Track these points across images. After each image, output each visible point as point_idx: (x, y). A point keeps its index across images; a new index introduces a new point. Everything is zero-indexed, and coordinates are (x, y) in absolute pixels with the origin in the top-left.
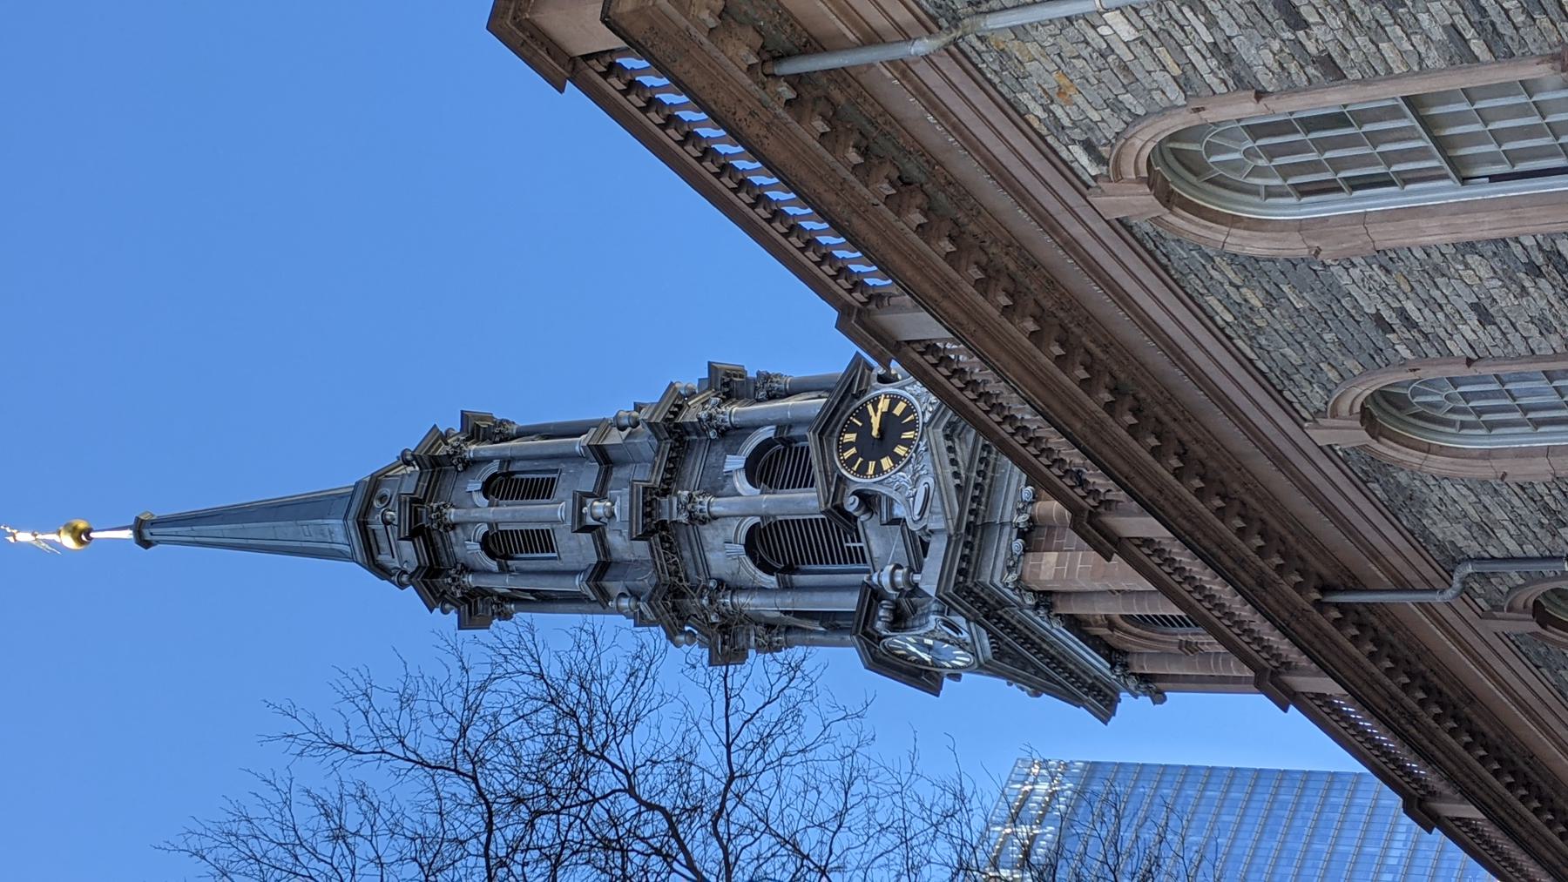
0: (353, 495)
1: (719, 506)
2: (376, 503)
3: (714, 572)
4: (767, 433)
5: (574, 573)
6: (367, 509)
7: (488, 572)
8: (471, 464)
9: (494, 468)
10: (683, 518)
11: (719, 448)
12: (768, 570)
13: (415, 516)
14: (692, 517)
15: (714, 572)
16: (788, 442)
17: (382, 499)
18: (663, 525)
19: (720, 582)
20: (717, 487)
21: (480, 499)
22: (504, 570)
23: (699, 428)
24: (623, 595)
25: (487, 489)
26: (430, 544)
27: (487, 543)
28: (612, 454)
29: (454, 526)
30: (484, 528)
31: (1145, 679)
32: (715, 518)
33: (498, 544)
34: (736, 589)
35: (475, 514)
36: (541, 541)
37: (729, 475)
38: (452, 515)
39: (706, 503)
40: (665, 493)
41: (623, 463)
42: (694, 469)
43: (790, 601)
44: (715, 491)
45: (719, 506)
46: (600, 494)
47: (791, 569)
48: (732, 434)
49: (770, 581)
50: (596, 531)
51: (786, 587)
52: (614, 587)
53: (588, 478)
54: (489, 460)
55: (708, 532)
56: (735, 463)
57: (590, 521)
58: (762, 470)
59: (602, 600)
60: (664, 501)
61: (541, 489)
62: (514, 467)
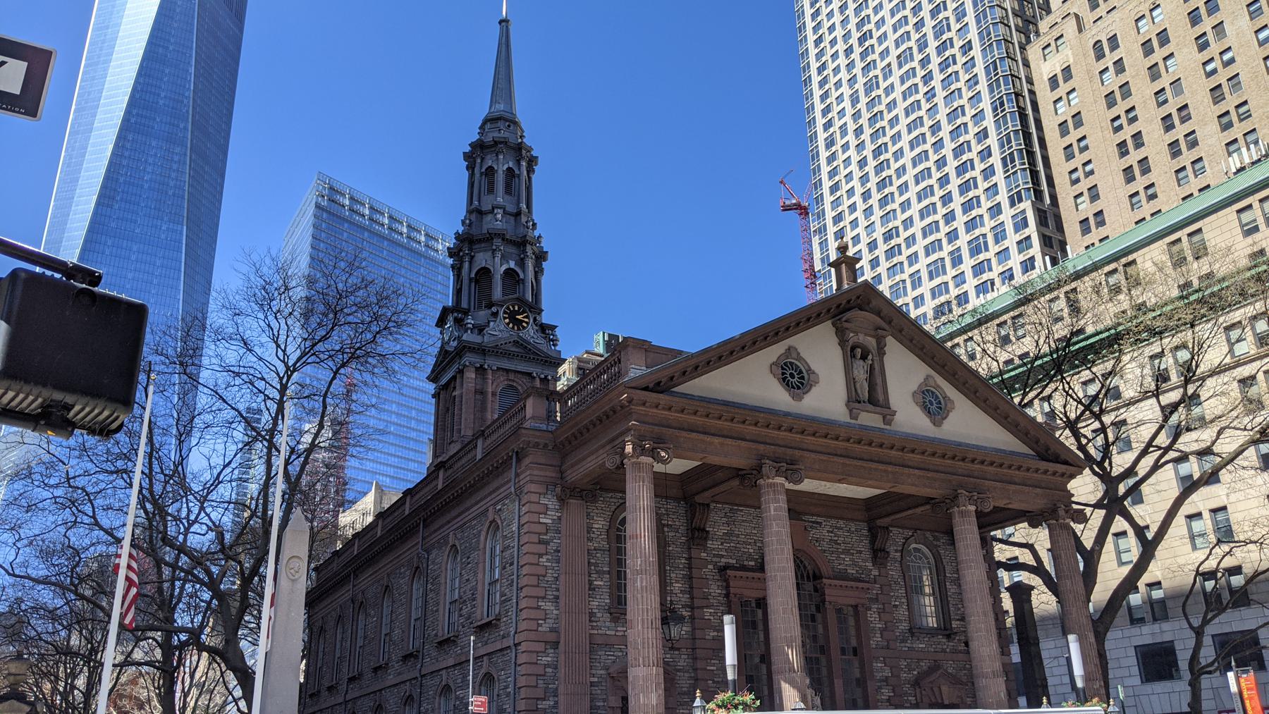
0: (512, 113)
1: (497, 260)
2: (507, 124)
3: (477, 255)
4: (522, 276)
5: (479, 201)
6: (506, 120)
7: (481, 168)
8: (518, 162)
9: (517, 172)
10: (494, 247)
11: (518, 258)
12: (476, 275)
13: (501, 143)
14: (494, 251)
15: (477, 255)
16: (518, 282)
17: (509, 126)
18: (492, 239)
19: (472, 257)
20: (504, 258)
21: (506, 167)
22: (481, 174)
23: (524, 252)
24: (470, 220)
25: (509, 169)
26: (491, 146)
27: (491, 168)
28: (518, 217)
29: (497, 156)
30: (496, 168)
31: (439, 394)
32: (494, 258)
33: (490, 172)
34: (471, 263)
35: (501, 165)
36: (491, 190)
37: (508, 262)
38: (501, 157)
39: (499, 255)
40: (503, 239)
41: (515, 220)
42: (512, 250)
43: (466, 282)
44: (503, 256)
45: (497, 260)
46: (505, 213)
47: (477, 282)
48: (522, 263)
49: (473, 275)
50: (492, 211)
51: (471, 280)
52: (473, 217)
53: (511, 208)
54: (519, 169)
55: (490, 253)
56: (512, 264)
57: (496, 211)
58: (509, 273)
59: (470, 212)
60: (500, 240)
61: (508, 189)
62: (517, 179)
